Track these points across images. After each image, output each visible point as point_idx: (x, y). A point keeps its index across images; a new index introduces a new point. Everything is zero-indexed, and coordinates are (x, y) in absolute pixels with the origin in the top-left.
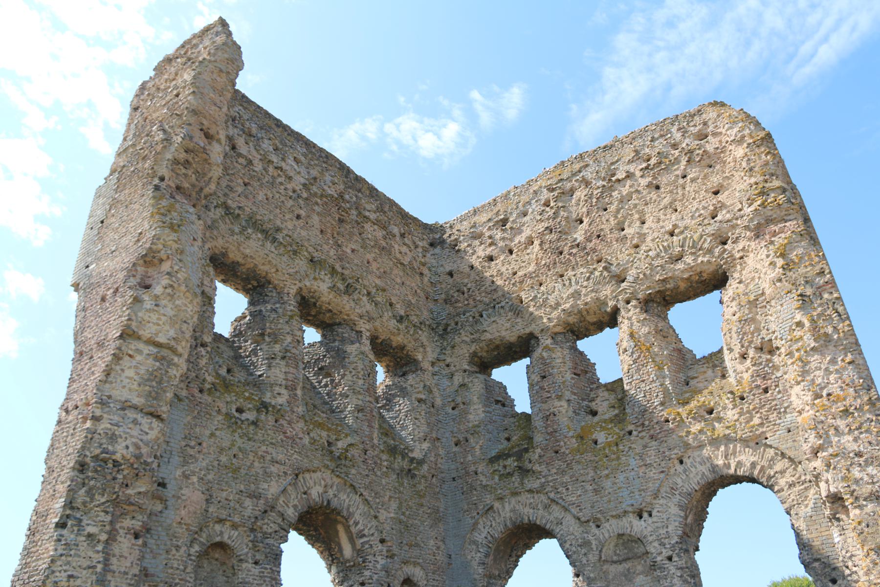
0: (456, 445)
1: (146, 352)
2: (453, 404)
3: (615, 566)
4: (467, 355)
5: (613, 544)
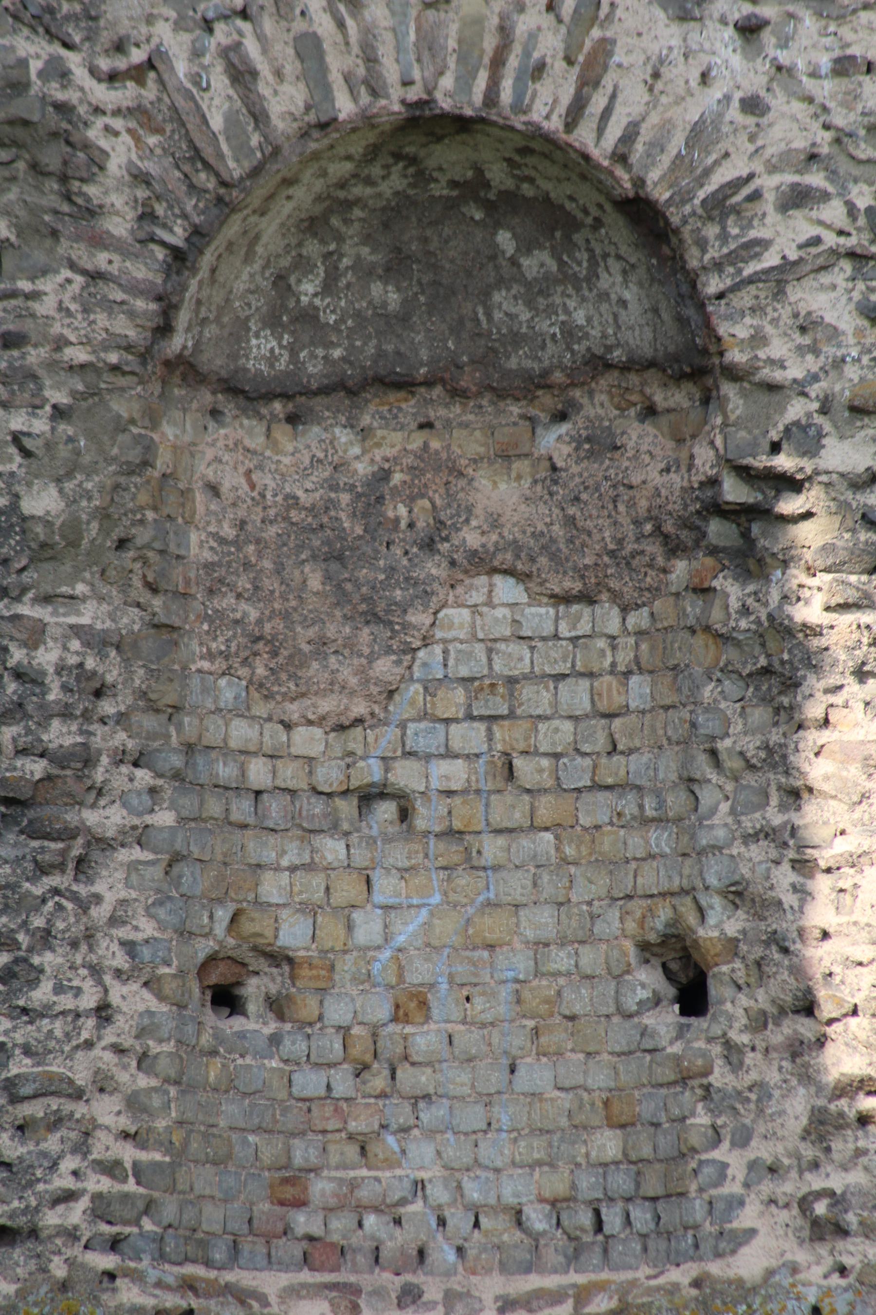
3: (247, 430)
5: (302, 198)
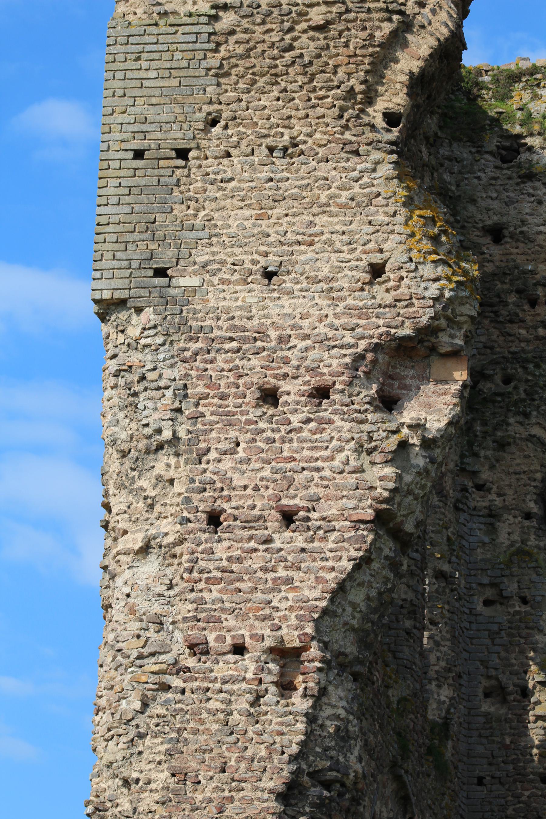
0: (487, 695)
1: (386, 551)
2: (489, 593)
4: (538, 476)
